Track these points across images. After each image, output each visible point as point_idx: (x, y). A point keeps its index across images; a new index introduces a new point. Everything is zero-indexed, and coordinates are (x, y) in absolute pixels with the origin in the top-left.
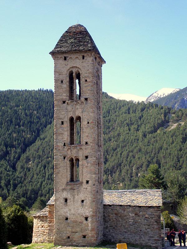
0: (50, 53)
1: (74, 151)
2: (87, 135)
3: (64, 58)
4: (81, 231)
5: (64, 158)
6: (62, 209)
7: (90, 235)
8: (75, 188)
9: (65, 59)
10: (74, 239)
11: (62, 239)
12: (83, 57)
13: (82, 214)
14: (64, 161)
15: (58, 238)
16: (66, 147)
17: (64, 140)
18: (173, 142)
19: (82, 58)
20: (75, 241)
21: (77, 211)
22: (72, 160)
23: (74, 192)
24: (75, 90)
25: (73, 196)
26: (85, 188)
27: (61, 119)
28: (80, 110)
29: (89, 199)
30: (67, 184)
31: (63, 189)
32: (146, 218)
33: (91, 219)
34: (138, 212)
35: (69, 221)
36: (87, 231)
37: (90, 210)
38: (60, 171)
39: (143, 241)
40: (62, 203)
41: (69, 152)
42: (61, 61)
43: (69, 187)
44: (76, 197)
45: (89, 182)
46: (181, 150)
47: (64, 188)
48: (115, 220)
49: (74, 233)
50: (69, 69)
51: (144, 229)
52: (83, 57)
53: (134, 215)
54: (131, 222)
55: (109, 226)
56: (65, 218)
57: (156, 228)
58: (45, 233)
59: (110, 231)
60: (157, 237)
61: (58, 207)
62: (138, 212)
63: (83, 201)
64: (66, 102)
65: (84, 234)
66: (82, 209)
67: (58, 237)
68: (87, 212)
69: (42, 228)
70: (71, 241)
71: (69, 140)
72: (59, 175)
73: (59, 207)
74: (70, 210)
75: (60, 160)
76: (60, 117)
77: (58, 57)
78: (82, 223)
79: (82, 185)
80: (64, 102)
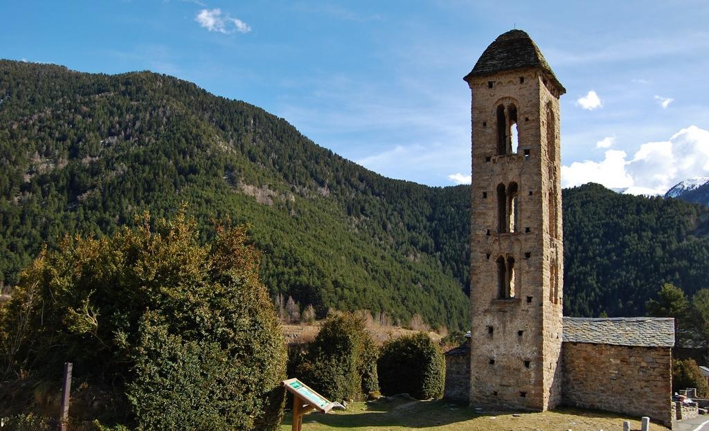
0: (466, 79)
1: (505, 244)
2: (528, 214)
3: (487, 84)
4: (517, 384)
5: (488, 256)
7: (533, 392)
8: (506, 310)
9: (490, 85)
10: (505, 398)
12: (522, 80)
13: (518, 355)
14: (487, 261)
16: (490, 237)
17: (488, 224)
19: (519, 82)
20: (506, 401)
21: (509, 349)
22: (500, 261)
24: (507, 139)
25: (503, 323)
26: (524, 310)
27: (482, 188)
28: (516, 172)
30: (493, 303)
31: (486, 311)
32: (643, 367)
33: (535, 365)
34: (628, 357)
35: (496, 366)
37: (534, 348)
38: (480, 279)
39: (635, 408)
41: (496, 246)
42: (484, 91)
43: (495, 308)
45: (532, 300)
47: (488, 309)
48: (582, 369)
49: (505, 388)
50: (497, 102)
51: (639, 387)
52: (522, 80)
53: (618, 362)
54: (613, 375)
55: (572, 378)
57: (662, 387)
59: (573, 388)
60: (663, 403)
61: (477, 342)
62: (628, 357)
63: (520, 333)
64: (492, 159)
65: (522, 390)
67: (478, 390)
68: (529, 351)
71: (496, 224)
72: (481, 285)
74: (498, 347)
75: (481, 260)
76: (481, 185)
77: (478, 84)
78: (520, 371)
79: (519, 304)
80: (488, 159)
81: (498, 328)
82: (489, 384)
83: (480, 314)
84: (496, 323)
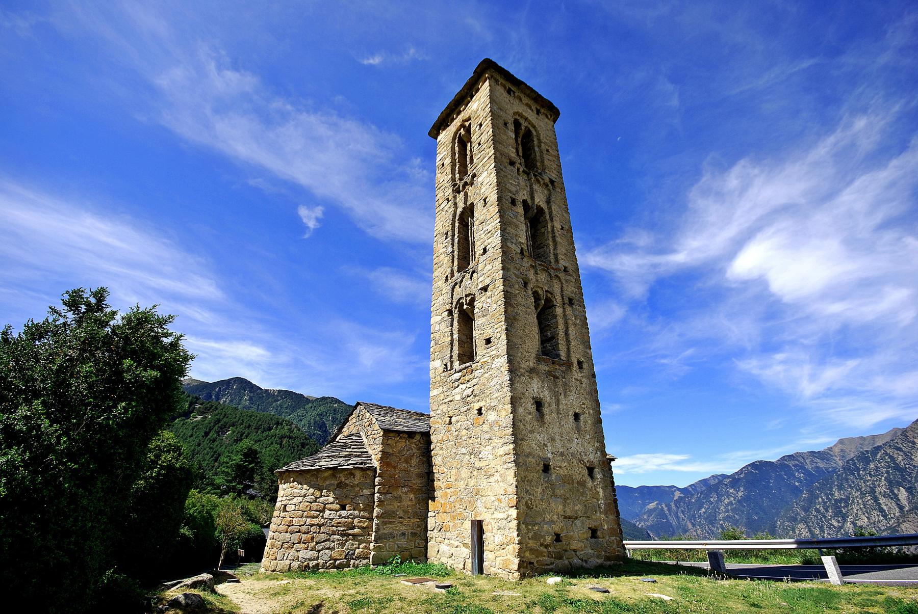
6: (532, 432)
11: (542, 545)
18: (191, 436)
20: (575, 551)
23: (556, 385)
26: (577, 380)
30: (538, 360)
31: (532, 371)
38: (517, 314)
40: (530, 414)
43: (544, 368)
44: (563, 401)
46: (199, 445)
58: (356, 530)
61: (522, 426)
63: (577, 416)
67: (530, 535)
69: (344, 513)
81: (549, 404)
84: (546, 395)
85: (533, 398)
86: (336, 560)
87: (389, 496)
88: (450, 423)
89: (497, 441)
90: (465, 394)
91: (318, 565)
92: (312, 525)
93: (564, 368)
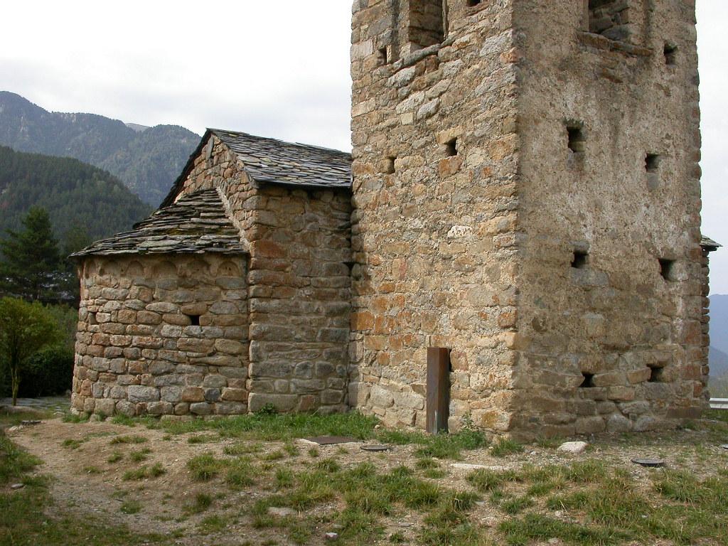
4: (647, 341)
6: (557, 189)
7: (679, 365)
8: (619, 74)
11: (556, 392)
15: (537, 386)
20: (616, 401)
23: (613, 96)
26: (659, 86)
29: (677, 154)
30: (581, 40)
35: (592, 277)
36: (669, 343)
40: (555, 153)
43: (591, 58)
49: (616, 355)
56: (570, 257)
58: (219, 359)
63: (650, 161)
65: (657, 358)
66: (652, 208)
67: (537, 374)
69: (195, 329)
70: (599, 400)
73: (541, 175)
74: (598, 206)
82: (573, 346)
83: (545, 72)
84: (591, 116)
85: (565, 122)
86: (190, 402)
87: (274, 303)
88: (392, 170)
89: (484, 205)
90: (422, 111)
91: (159, 407)
92: (142, 347)
93: (633, 61)
